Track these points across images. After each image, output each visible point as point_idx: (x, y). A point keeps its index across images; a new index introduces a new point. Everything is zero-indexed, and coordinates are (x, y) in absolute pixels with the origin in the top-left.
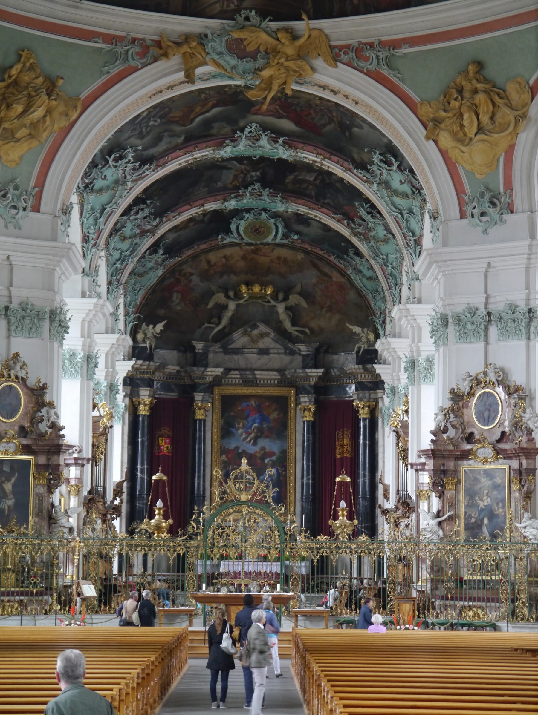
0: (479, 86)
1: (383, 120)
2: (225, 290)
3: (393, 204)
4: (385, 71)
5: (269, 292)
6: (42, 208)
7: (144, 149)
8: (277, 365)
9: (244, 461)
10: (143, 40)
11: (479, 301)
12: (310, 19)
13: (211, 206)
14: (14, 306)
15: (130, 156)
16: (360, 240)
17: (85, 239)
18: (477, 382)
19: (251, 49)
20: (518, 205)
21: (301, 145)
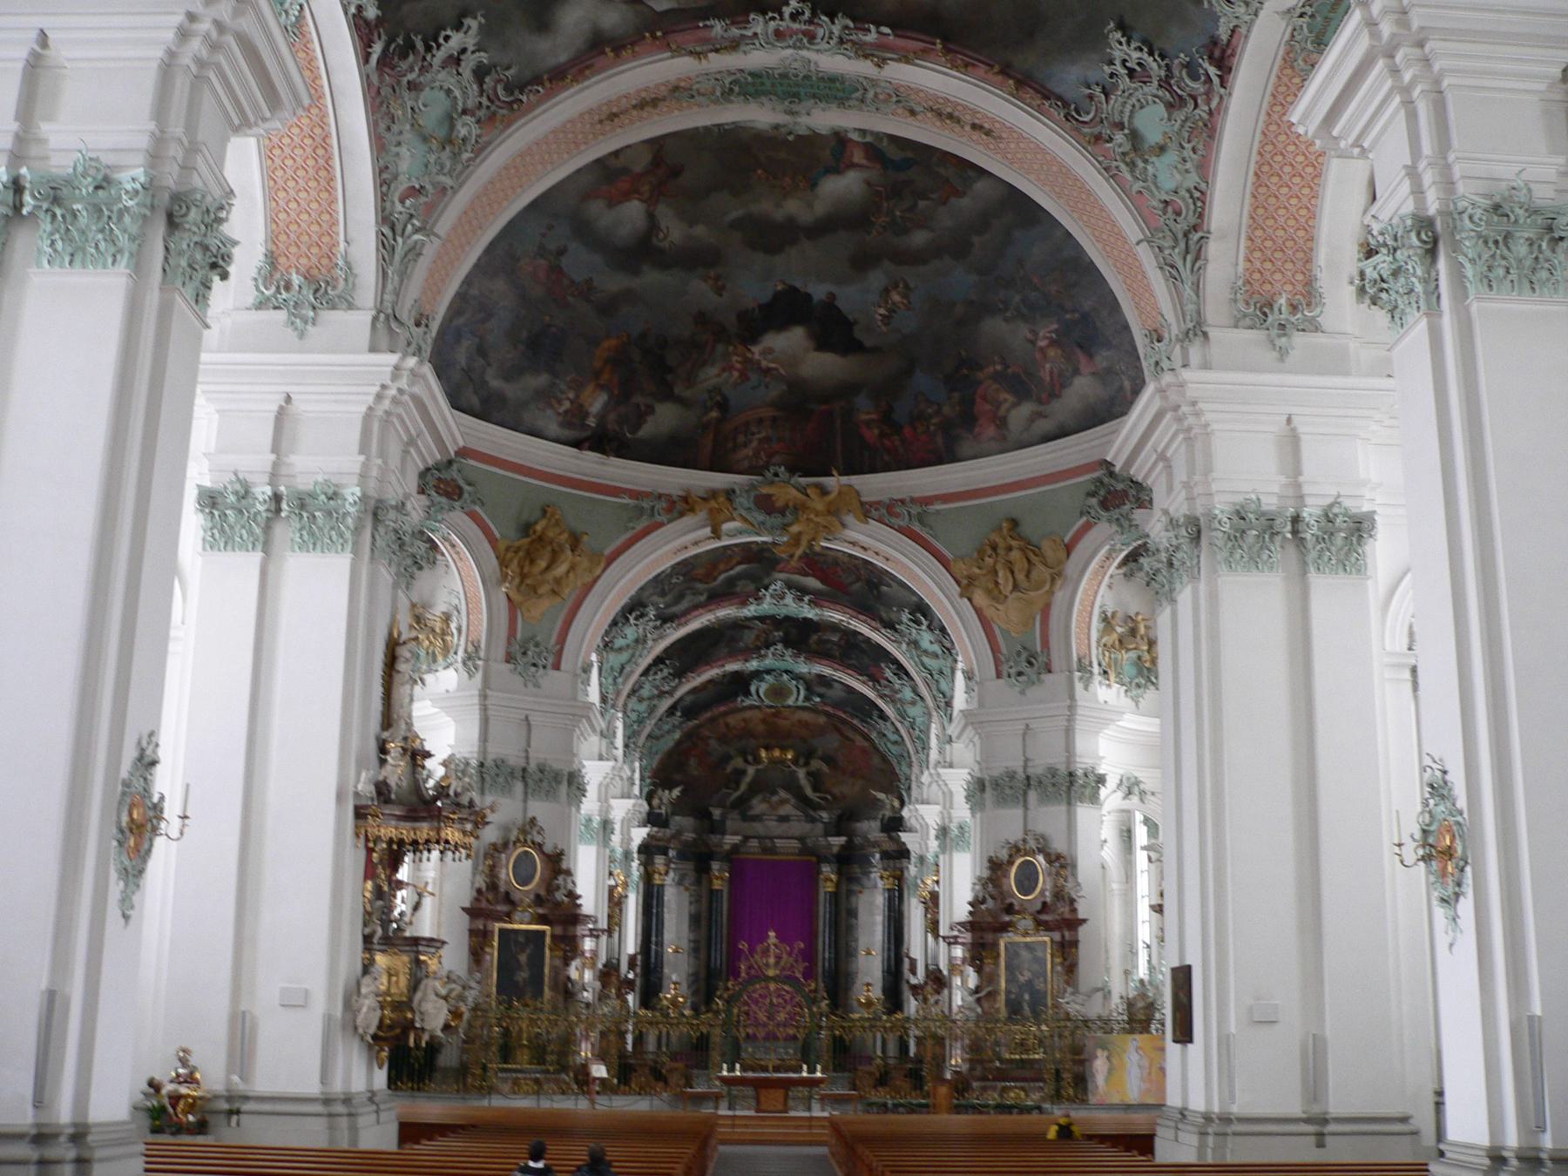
0: (1014, 543)
1: (915, 577)
2: (743, 753)
3: (923, 665)
4: (916, 527)
5: (789, 757)
6: (563, 665)
7: (667, 606)
8: (797, 833)
9: (772, 934)
11: (1017, 765)
12: (840, 475)
13: (733, 667)
14: (532, 767)
15: (652, 613)
16: (886, 702)
17: (604, 699)
18: (1016, 850)
19: (780, 504)
20: (1055, 665)
21: (827, 604)
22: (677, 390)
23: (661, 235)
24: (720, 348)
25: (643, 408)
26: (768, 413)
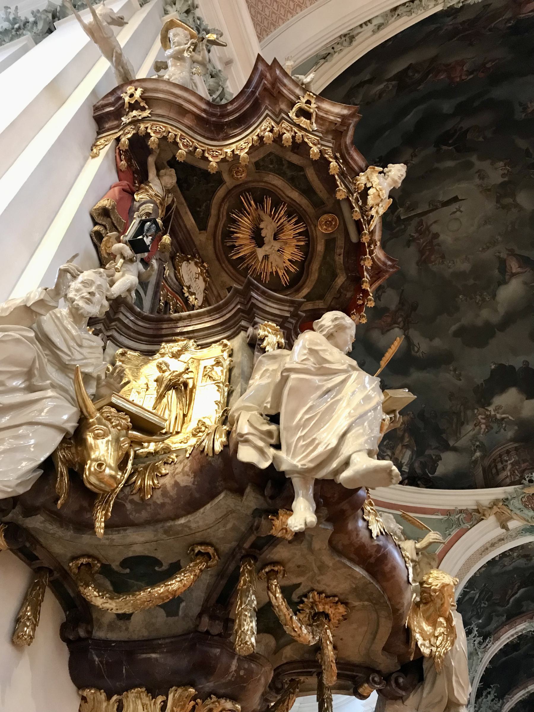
10: (467, 510)
22: (451, 443)
23: (416, 349)
24: (469, 413)
25: (434, 457)
26: (511, 446)
